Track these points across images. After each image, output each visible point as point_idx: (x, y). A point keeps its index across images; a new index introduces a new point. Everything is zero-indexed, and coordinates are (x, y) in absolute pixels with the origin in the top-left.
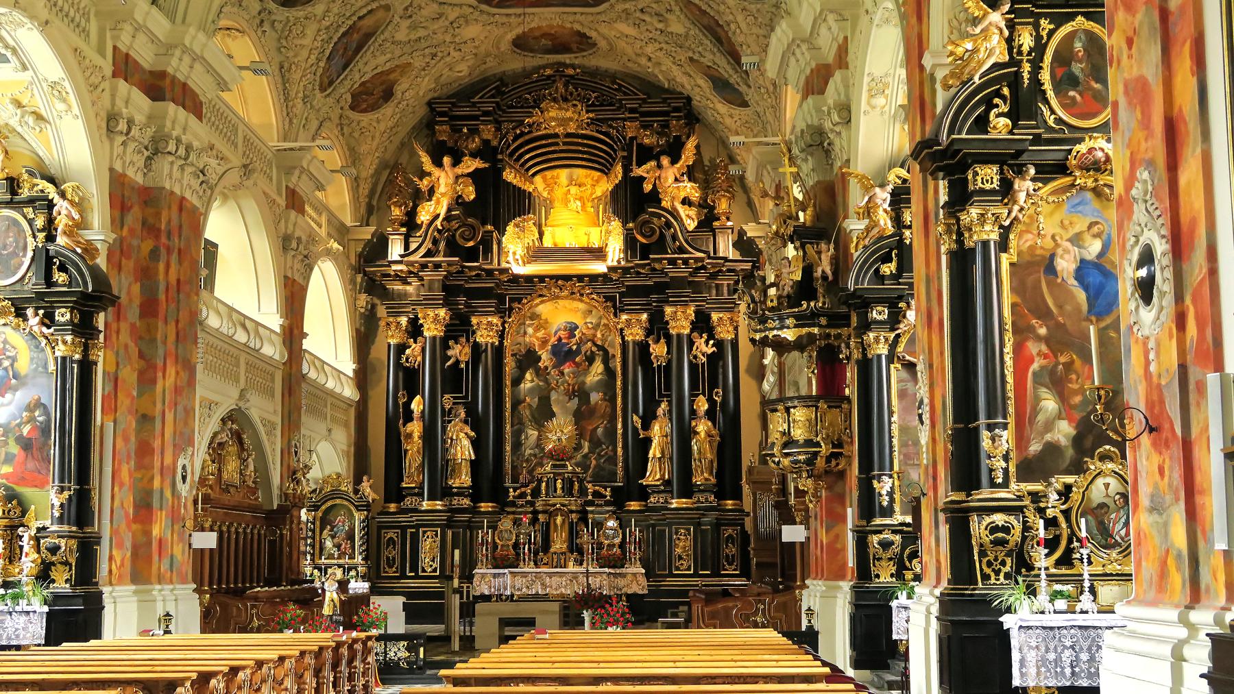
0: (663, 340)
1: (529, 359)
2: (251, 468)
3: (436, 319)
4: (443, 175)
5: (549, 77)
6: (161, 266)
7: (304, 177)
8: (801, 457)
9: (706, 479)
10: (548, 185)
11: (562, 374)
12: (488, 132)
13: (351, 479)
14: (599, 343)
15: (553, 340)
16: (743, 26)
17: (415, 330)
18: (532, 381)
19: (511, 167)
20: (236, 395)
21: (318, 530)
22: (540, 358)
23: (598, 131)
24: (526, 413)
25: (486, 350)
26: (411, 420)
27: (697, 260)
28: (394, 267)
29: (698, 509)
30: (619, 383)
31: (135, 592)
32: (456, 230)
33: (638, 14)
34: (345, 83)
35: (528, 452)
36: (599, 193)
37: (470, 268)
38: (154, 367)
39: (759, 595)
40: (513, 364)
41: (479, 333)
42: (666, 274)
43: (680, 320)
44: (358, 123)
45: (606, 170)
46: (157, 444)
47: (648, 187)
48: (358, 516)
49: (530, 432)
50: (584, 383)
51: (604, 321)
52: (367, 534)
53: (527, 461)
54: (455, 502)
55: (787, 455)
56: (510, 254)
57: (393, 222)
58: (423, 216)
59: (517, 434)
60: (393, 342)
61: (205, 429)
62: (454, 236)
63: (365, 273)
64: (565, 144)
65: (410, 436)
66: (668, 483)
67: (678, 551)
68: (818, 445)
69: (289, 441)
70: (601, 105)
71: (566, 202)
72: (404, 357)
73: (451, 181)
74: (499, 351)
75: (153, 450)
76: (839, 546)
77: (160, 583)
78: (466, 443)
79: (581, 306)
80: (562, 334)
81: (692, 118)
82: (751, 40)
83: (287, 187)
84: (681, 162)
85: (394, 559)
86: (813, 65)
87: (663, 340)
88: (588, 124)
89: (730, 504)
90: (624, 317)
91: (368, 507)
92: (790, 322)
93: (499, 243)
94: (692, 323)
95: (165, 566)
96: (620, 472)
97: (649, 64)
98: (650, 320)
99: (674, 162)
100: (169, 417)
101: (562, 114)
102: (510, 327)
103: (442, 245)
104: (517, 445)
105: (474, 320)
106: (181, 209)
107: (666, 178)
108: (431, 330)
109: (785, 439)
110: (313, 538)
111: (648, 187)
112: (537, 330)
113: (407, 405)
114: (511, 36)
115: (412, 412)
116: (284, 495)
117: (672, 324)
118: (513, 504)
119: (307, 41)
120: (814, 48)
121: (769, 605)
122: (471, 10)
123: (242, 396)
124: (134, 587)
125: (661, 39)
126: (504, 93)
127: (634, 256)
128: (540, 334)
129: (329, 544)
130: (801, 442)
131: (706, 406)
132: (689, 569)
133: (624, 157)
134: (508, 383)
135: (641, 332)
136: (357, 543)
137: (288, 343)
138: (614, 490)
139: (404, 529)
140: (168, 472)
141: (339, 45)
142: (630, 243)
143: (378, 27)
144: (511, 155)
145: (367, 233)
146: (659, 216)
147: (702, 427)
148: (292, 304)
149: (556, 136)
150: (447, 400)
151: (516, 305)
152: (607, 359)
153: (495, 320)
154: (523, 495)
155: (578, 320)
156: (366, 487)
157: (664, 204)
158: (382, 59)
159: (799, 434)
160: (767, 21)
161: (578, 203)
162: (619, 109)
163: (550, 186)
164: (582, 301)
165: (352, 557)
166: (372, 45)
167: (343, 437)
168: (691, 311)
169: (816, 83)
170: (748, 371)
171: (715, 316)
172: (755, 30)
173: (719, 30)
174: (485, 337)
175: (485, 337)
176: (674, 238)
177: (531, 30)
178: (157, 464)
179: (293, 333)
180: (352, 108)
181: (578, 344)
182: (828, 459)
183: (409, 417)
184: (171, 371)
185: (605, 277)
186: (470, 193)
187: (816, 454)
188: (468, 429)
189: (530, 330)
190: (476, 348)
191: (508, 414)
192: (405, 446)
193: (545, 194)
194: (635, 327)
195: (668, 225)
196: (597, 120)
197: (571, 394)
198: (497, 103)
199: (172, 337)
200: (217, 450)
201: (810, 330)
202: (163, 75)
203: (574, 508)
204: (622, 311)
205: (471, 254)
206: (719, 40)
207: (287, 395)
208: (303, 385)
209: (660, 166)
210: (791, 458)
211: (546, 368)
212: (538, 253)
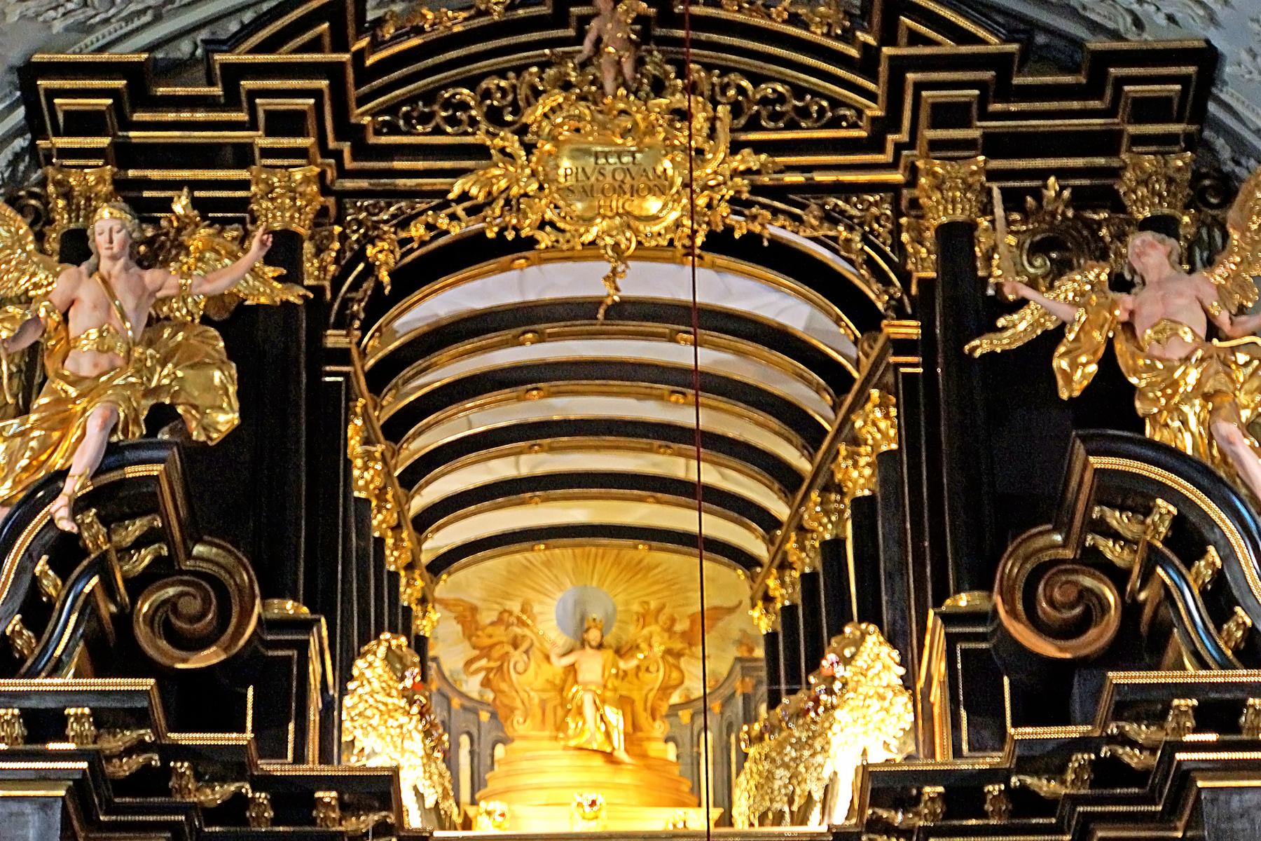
4: (89, 291)
10: (486, 651)
32: (138, 585)
42: (1185, 777)
47: (1075, 373)
62: (124, 619)
71: (559, 710)
93: (329, 708)
103: (67, 626)
111: (1075, 373)
133: (902, 346)
162: (874, 143)
193: (472, 686)
195: (1188, 539)
196: (779, 192)
205: (200, 700)
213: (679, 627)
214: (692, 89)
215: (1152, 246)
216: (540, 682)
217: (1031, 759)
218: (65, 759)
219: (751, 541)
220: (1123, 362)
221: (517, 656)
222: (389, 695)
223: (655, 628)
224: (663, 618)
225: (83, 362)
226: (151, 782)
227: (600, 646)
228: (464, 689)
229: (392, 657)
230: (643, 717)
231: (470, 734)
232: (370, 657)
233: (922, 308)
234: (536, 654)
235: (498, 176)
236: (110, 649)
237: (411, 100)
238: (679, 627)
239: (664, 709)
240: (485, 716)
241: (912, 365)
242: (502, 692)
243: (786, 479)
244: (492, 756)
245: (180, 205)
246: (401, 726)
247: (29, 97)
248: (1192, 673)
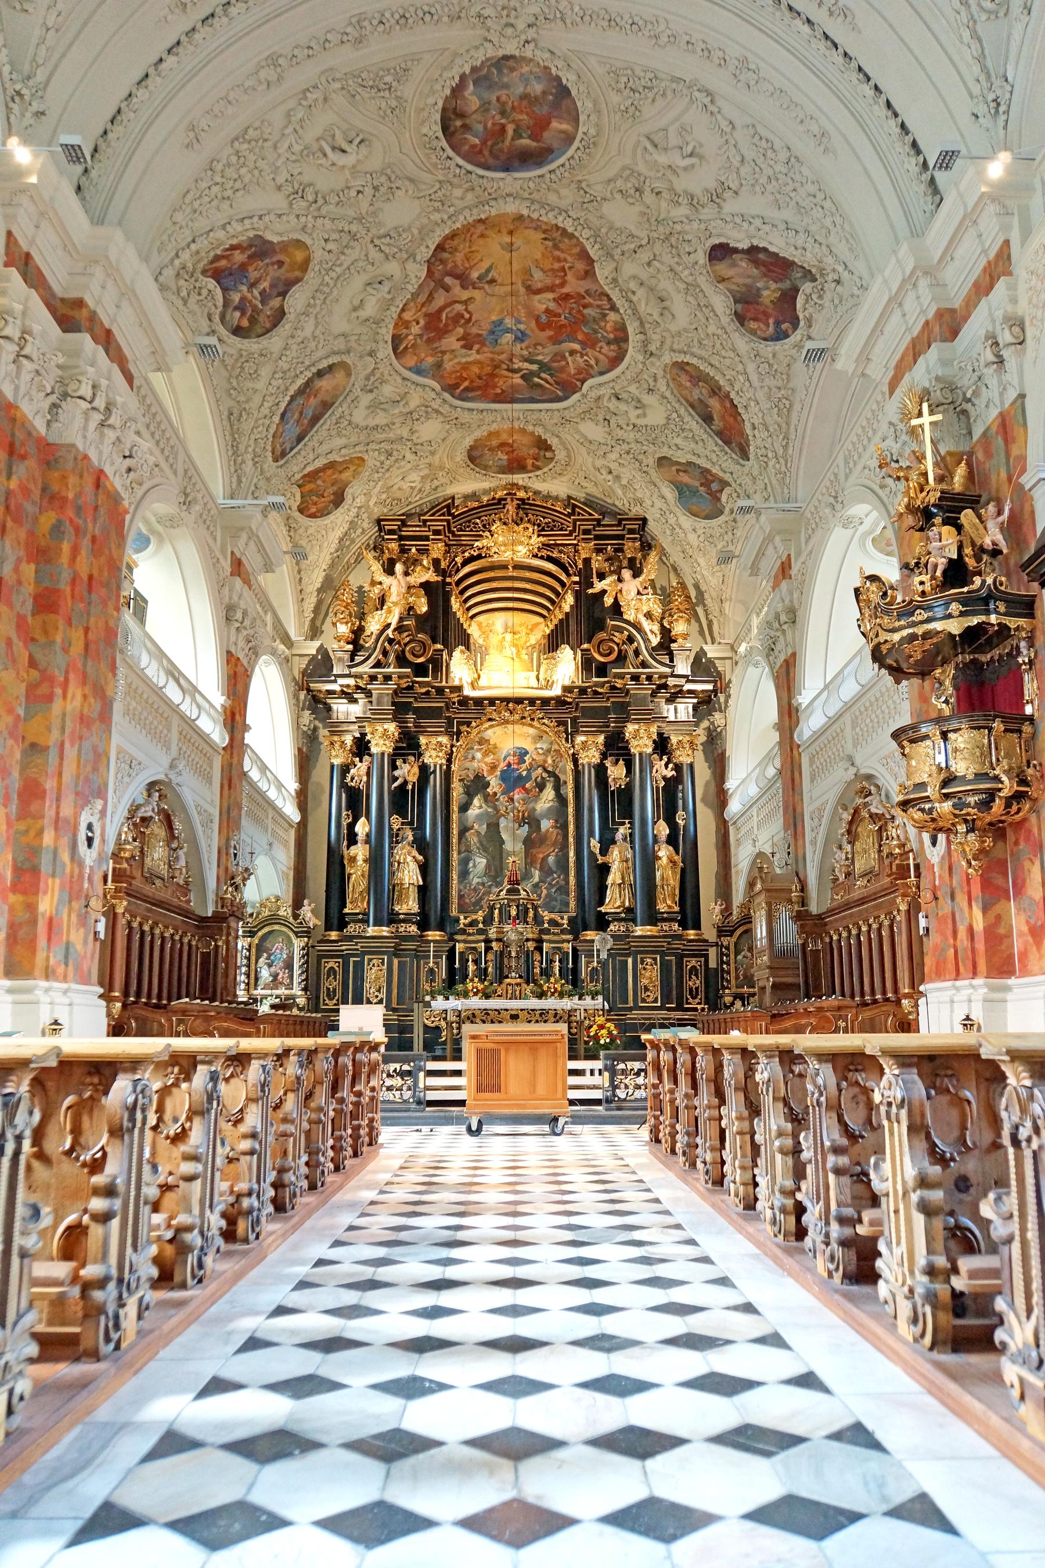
0: (621, 762)
1: (477, 785)
2: (182, 863)
3: (385, 734)
5: (500, 500)
6: (66, 547)
7: (252, 544)
8: (972, 799)
9: (669, 907)
11: (512, 800)
12: (437, 550)
13: (290, 902)
14: (550, 769)
15: (502, 765)
16: (754, 378)
17: (361, 747)
18: (481, 807)
20: (165, 761)
21: (253, 958)
22: (488, 784)
23: (550, 559)
24: (472, 838)
25: (434, 772)
26: (355, 843)
27: (663, 676)
28: (341, 681)
29: (665, 937)
30: (571, 810)
31: (10, 991)
32: (406, 645)
33: (613, 404)
34: (300, 458)
35: (476, 880)
36: (533, 642)
38: (51, 680)
39: (839, 1008)
40: (461, 790)
41: (427, 754)
42: (628, 691)
43: (640, 739)
44: (307, 529)
46: (50, 784)
47: (608, 601)
48: (298, 944)
49: (478, 860)
50: (534, 810)
51: (556, 747)
52: (307, 962)
53: (475, 890)
54: (401, 929)
55: (947, 796)
57: (338, 639)
58: (373, 625)
59: (465, 862)
60: (337, 762)
61: (123, 795)
62: (403, 651)
63: (309, 690)
65: (353, 859)
66: (630, 910)
67: (645, 981)
68: (997, 779)
69: (228, 840)
71: (501, 647)
72: (349, 776)
73: (404, 590)
74: (447, 775)
75: (44, 791)
76: (1002, 931)
77: (47, 978)
78: (413, 867)
79: (532, 731)
80: (511, 759)
81: (647, 547)
82: (761, 395)
83: (232, 553)
85: (334, 990)
86: (930, 314)
87: (621, 762)
88: (539, 549)
89: (691, 934)
90: (580, 739)
91: (308, 933)
92: (955, 608)
93: (448, 666)
94: (654, 741)
95: (56, 957)
96: (572, 904)
97: (610, 477)
98: (607, 744)
99: (636, 574)
100: (71, 752)
102: (458, 752)
103: (392, 657)
104: (464, 874)
105: (423, 740)
106: (98, 485)
108: (380, 746)
109: (942, 776)
110: (248, 966)
111: (608, 601)
112: (486, 754)
113: (351, 826)
114: (468, 442)
115: (356, 835)
116: (221, 900)
117: (633, 743)
118: (463, 932)
119: (260, 385)
120: (937, 284)
121: (852, 1022)
122: (433, 395)
123: (172, 766)
124: (7, 983)
125: (631, 436)
127: (589, 676)
128: (489, 759)
129: (265, 974)
130: (970, 777)
131: (668, 831)
132: (656, 1001)
133: (575, 583)
134: (456, 809)
135: (597, 755)
136: (297, 971)
137: (229, 727)
138: (570, 920)
139: (346, 958)
140: (65, 826)
141: (295, 404)
142: (587, 664)
143: (337, 397)
144: (458, 583)
145: (311, 648)
146: (620, 630)
147: (664, 852)
148: (235, 685)
150: (396, 822)
151: (464, 728)
152: (558, 787)
153: (444, 740)
154: (473, 923)
155: (528, 745)
156: (306, 911)
158: (340, 442)
159: (961, 767)
160: (782, 368)
161: (514, 650)
162: (570, 535)
163: (486, 632)
164: (531, 726)
165: (290, 986)
166: (328, 421)
167: (286, 857)
168: (654, 729)
169: (949, 324)
170: (703, 800)
171: (674, 740)
172: (769, 381)
173: (714, 403)
174: (433, 758)
175: (433, 758)
176: (637, 652)
177: (490, 434)
178: (50, 813)
179: (235, 719)
180: (301, 510)
181: (528, 770)
182: (1009, 802)
183: (352, 839)
184: (75, 691)
185: (560, 701)
187: (992, 794)
188: (415, 853)
189: (479, 755)
190: (424, 769)
191: (455, 840)
192: (348, 870)
193: (481, 641)
194: (590, 748)
195: (631, 639)
196: (549, 545)
197: (521, 821)
198: (448, 521)
199: (77, 648)
200: (139, 824)
201: (982, 618)
202: (79, 303)
203: (530, 936)
204: (576, 732)
205: (420, 670)
206: (707, 419)
207: (226, 787)
208: (244, 783)
209: (620, 580)
210: (950, 803)
211: (495, 794)
214: (529, 521)
217: (596, 684)
218: (392, 685)
219: (545, 612)
226: (410, 688)
229: (462, 652)
233: (579, 575)
235: (485, 542)
236: (402, 660)
241: (577, 587)
243: (553, 602)
245: (414, 550)
248: (632, 670)
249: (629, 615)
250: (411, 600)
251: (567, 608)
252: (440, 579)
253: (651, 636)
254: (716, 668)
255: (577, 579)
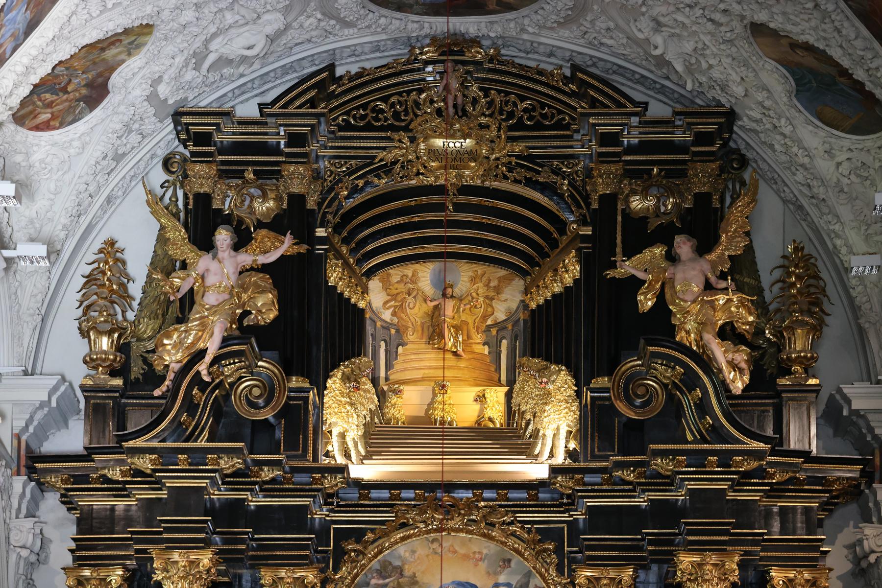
4: (214, 266)
10: (394, 297)
19: (339, 256)
23: (530, 183)
36: (501, 316)
37: (260, 464)
45: (530, 263)
47: (646, 302)
56: (335, 440)
64: (458, 207)
70: (538, 126)
81: (734, 162)
84: (718, 251)
99: (704, 248)
101: (454, 144)
107: (687, 283)
111: (646, 302)
126: (333, 96)
133: (585, 238)
149: (441, 190)
157: (680, 336)
176: (703, 407)
186: (265, 307)
193: (387, 316)
195: (690, 382)
196: (530, 158)
209: (672, 258)
212: (380, 437)
213: (492, 284)
215: (684, 243)
216: (420, 314)
220: (668, 296)
221: (410, 299)
222: (343, 396)
223: (480, 285)
224: (484, 279)
225: (211, 299)
227: (452, 297)
228: (383, 317)
230: (473, 332)
231: (385, 341)
232: (334, 379)
234: (420, 298)
237: (357, 108)
238: (492, 284)
239: (484, 327)
240: (393, 331)
242: (403, 319)
244: (397, 352)
246: (348, 412)
247: (176, 123)
249: (688, 332)
250: (245, 297)
251: (568, 280)
252: (303, 248)
253: (730, 375)
254: (871, 430)
255: (587, 231)
